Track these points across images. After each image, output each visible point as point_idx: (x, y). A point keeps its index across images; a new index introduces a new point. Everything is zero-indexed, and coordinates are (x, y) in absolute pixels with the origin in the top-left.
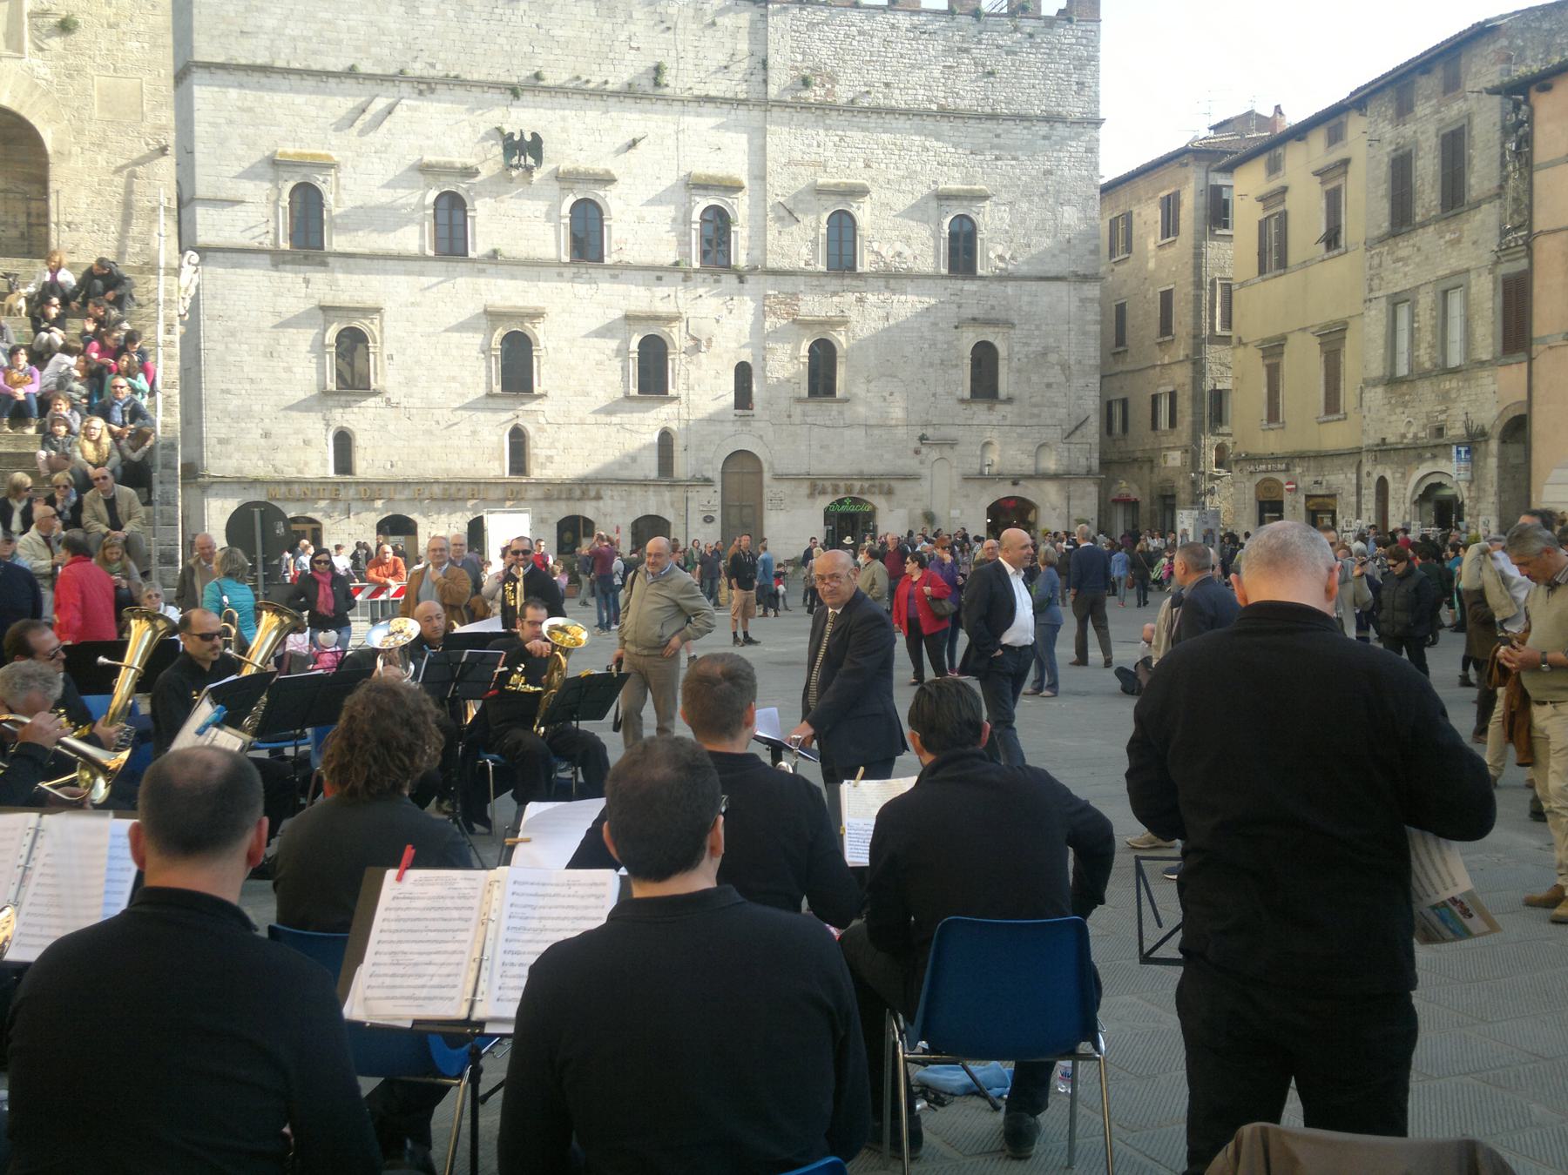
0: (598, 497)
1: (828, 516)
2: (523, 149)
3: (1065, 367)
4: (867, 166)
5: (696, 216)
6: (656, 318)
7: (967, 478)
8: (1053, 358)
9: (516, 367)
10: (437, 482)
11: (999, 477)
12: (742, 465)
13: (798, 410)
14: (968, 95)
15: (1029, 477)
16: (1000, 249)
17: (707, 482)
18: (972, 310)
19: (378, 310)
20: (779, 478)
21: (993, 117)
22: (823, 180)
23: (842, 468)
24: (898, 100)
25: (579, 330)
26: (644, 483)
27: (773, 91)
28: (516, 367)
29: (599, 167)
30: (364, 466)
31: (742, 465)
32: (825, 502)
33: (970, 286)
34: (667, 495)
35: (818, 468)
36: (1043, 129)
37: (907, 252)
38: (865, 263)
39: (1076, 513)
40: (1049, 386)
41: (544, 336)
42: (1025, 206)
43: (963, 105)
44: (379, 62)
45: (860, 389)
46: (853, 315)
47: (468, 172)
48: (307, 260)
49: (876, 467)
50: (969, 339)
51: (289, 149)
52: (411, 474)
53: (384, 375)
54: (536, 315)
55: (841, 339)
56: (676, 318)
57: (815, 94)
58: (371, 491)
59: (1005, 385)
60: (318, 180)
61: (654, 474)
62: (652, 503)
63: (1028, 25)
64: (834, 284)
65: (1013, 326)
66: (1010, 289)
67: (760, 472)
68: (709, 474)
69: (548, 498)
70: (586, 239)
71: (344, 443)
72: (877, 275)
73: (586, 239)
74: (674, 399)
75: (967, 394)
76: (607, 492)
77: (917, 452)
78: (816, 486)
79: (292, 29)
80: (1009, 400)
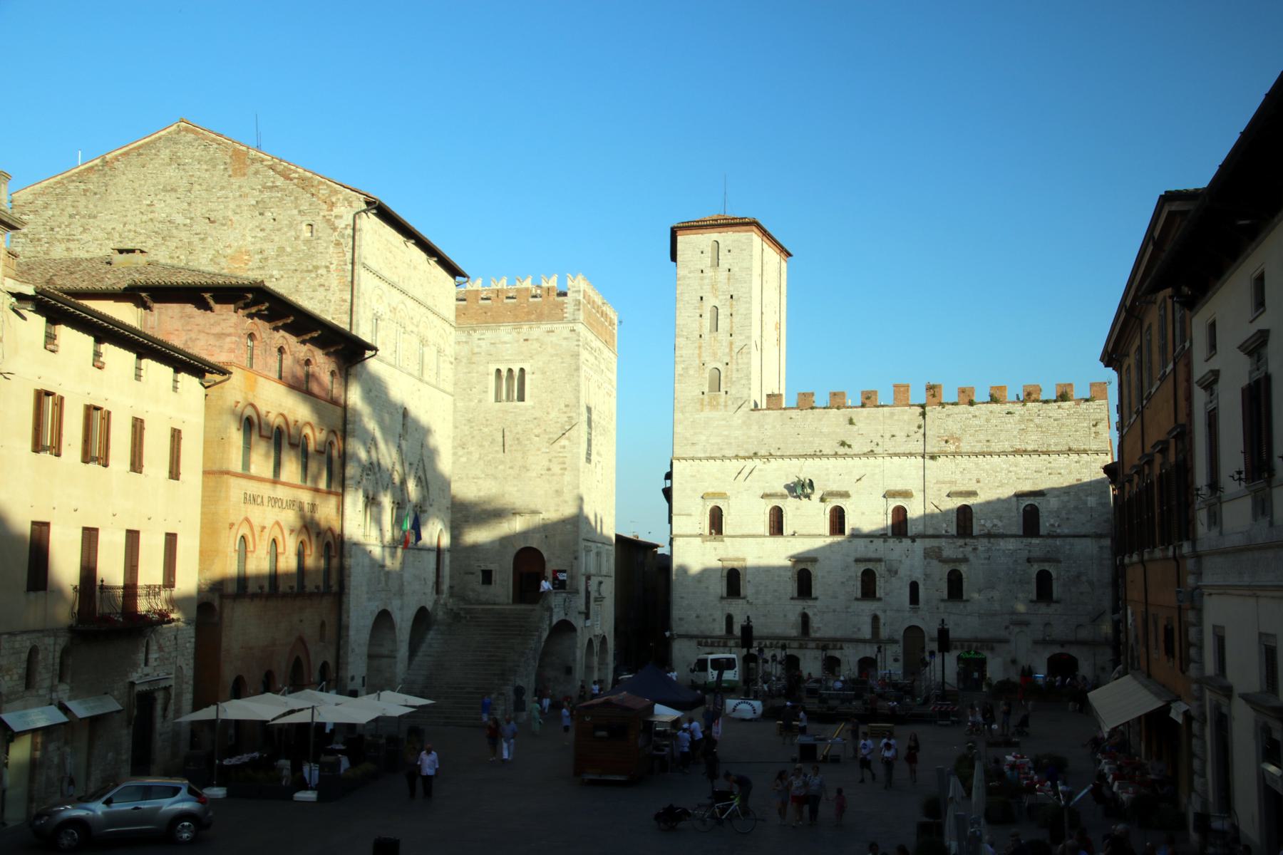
0: (841, 648)
4: (978, 482)
5: (890, 511)
6: (869, 560)
7: (1036, 642)
8: (1084, 578)
10: (767, 638)
11: (1053, 642)
12: (913, 634)
13: (942, 605)
15: (1071, 643)
16: (1052, 521)
17: (896, 642)
18: (1037, 553)
21: (1047, 453)
22: (954, 489)
24: (996, 447)
26: (864, 641)
27: (929, 449)
29: (843, 489)
33: (1035, 541)
37: (1000, 524)
38: (976, 531)
40: (1082, 593)
43: (1029, 448)
44: (747, 451)
45: (976, 596)
46: (971, 557)
50: (1036, 568)
51: (710, 490)
55: (963, 569)
56: (880, 560)
57: (951, 448)
59: (1057, 591)
60: (720, 503)
61: (868, 636)
62: (869, 651)
64: (961, 542)
65: (1059, 562)
66: (1058, 542)
67: (924, 637)
68: (897, 637)
71: (729, 619)
72: (984, 536)
74: (880, 599)
75: (1034, 598)
76: (845, 645)
77: (1007, 628)
79: (713, 440)
80: (1057, 602)
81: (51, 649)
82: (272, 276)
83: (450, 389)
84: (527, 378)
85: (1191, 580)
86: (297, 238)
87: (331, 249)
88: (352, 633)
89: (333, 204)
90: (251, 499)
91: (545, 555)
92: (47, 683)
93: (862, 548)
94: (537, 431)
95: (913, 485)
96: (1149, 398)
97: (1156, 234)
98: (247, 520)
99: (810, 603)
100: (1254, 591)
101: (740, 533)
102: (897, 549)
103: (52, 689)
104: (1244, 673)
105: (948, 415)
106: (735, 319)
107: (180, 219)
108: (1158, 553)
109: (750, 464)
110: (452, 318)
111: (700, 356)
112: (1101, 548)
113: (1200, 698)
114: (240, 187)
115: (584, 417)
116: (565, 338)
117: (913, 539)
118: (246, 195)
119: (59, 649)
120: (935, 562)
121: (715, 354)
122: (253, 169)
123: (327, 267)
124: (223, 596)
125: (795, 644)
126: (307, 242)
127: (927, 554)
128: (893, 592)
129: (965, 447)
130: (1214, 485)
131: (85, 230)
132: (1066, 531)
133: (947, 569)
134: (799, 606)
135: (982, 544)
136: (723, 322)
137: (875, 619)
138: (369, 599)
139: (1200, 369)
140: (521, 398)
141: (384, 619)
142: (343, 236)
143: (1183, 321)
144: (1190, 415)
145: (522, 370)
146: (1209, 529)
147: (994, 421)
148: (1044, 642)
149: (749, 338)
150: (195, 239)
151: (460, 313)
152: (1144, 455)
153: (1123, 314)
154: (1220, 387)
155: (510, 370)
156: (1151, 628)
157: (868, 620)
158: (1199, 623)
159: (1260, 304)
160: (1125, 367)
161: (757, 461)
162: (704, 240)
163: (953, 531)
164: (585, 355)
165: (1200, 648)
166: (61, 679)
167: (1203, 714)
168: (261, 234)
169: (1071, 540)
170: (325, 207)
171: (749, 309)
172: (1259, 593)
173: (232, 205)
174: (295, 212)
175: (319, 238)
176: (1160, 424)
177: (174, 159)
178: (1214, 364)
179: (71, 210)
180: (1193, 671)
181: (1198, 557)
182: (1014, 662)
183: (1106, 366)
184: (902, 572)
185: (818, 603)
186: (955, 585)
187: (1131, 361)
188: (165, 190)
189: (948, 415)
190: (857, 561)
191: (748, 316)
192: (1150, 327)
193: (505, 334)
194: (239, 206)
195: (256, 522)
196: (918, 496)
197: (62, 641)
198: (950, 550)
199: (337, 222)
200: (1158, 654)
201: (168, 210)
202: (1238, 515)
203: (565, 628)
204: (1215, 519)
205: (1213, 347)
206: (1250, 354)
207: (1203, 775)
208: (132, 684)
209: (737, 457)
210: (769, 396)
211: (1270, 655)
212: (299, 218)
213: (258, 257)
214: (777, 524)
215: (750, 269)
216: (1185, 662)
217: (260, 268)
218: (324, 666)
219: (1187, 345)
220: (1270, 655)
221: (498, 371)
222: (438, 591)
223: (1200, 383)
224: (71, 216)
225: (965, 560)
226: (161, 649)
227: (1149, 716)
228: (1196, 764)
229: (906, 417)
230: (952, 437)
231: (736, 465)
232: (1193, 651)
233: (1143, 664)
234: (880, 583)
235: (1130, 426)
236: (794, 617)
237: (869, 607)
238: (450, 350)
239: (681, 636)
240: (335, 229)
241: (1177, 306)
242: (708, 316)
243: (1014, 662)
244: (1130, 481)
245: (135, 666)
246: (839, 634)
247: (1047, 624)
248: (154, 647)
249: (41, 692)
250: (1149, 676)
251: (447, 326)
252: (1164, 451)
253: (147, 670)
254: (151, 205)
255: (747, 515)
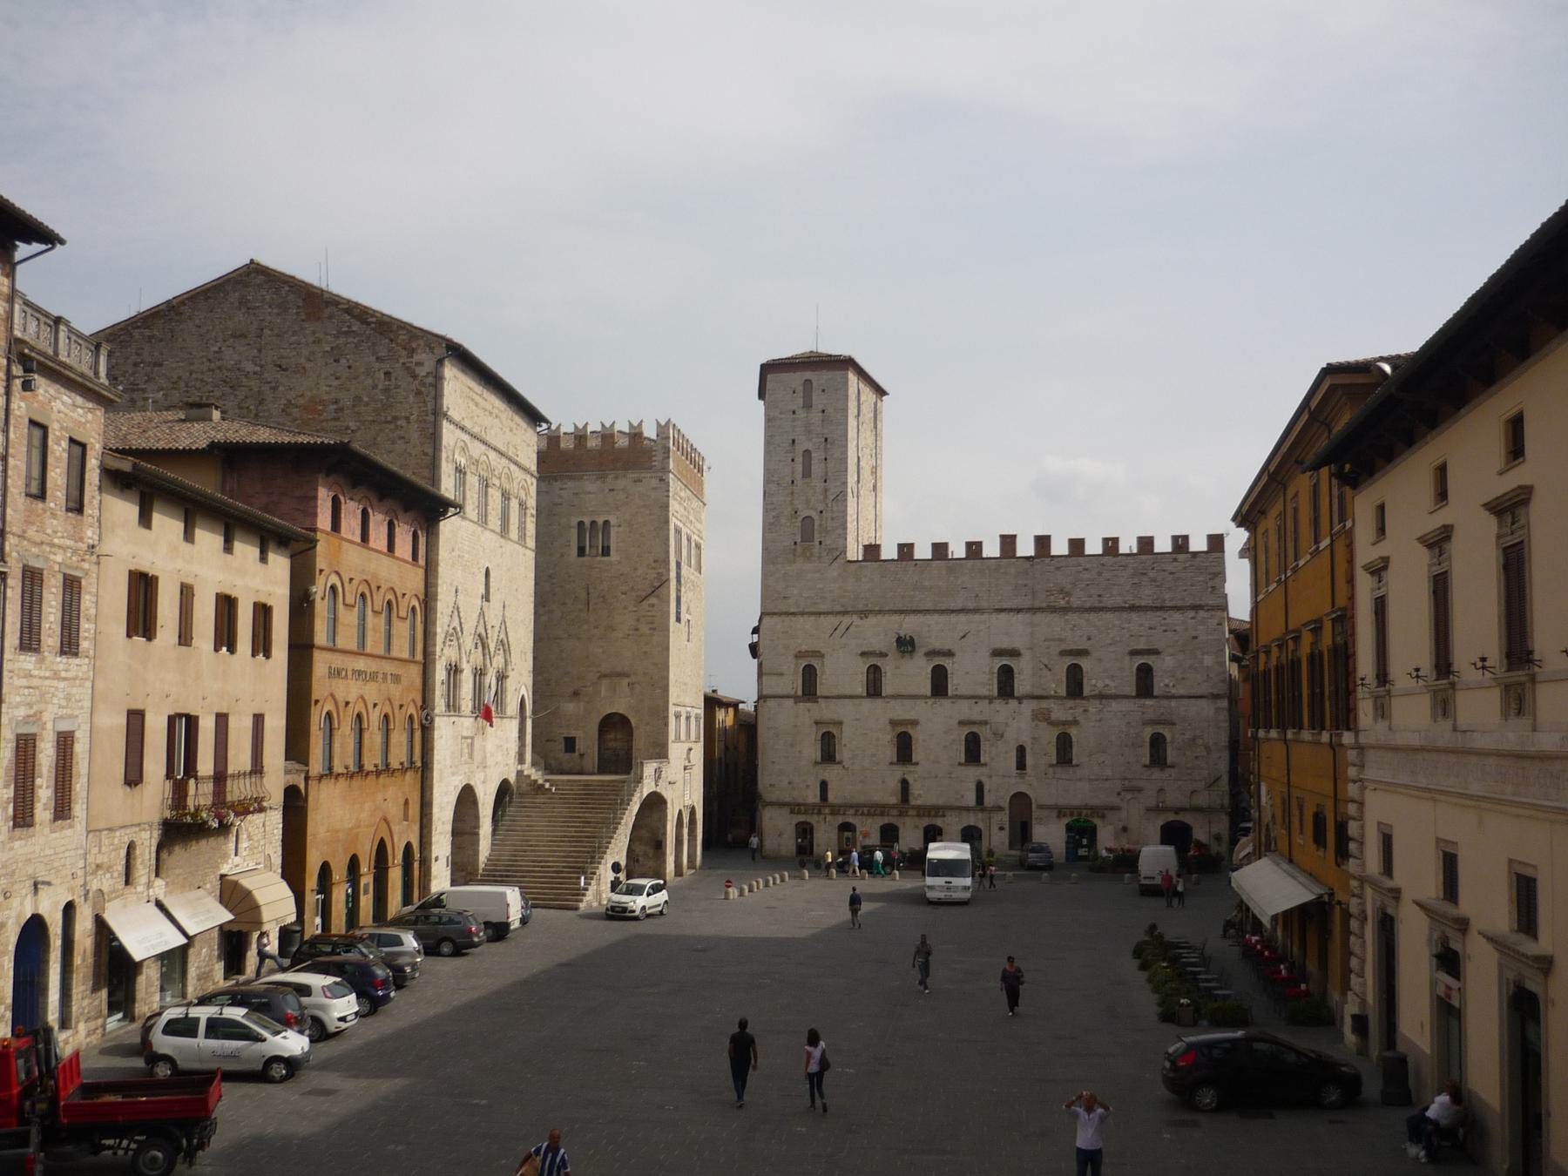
1: (1069, 828)
2: (906, 645)
3: (1207, 748)
6: (973, 723)
7: (1149, 810)
8: (1200, 742)
9: (904, 748)
10: (865, 806)
12: (1021, 802)
14: (1147, 596)
17: (1000, 809)
18: (1151, 715)
19: (841, 723)
20: (1041, 807)
21: (1161, 608)
22: (1064, 647)
23: (1076, 802)
24: (1109, 603)
25: (938, 729)
26: (967, 809)
28: (904, 748)
30: (831, 798)
31: (1021, 802)
32: (1067, 820)
33: (1149, 702)
34: (980, 815)
35: (1062, 802)
36: (1191, 614)
38: (1086, 692)
39: (1215, 830)
41: (918, 735)
42: (1181, 657)
43: (1143, 603)
46: (1081, 718)
47: (883, 655)
48: (809, 701)
49: (1096, 802)
50: (1148, 732)
51: (804, 648)
52: (854, 801)
53: (843, 753)
54: (915, 723)
55: (1073, 732)
56: (986, 723)
58: (836, 810)
59: (1171, 755)
60: (815, 663)
62: (971, 820)
63: (1181, 557)
64: (1070, 703)
66: (1173, 703)
69: (918, 815)
70: (939, 684)
71: (824, 786)
72: (1094, 697)
73: (939, 684)
76: (948, 813)
78: (1061, 812)
80: (1172, 766)
81: (148, 841)
82: (348, 428)
83: (531, 543)
84: (613, 531)
85: (1352, 772)
86: (375, 387)
87: (411, 399)
88: (435, 810)
89: (413, 350)
90: (336, 673)
91: (633, 722)
92: (144, 880)
93: (966, 710)
94: (624, 588)
95: (1018, 643)
96: (1295, 570)
97: (1313, 404)
98: (332, 695)
99: (911, 768)
100: (1433, 794)
101: (835, 692)
102: (1001, 712)
103: (149, 885)
104: (1417, 877)
105: (1058, 568)
106: (831, 464)
107: (249, 367)
108: (1306, 735)
109: (847, 620)
110: (534, 468)
111: (792, 503)
112: (1218, 709)
113: (1360, 896)
114: (314, 332)
115: (673, 575)
116: (654, 489)
117: (1020, 700)
118: (318, 341)
119: (155, 842)
120: (1043, 725)
121: (808, 502)
122: (327, 311)
123: (407, 419)
124: (307, 778)
125: (894, 812)
126: (386, 390)
127: (1039, 716)
128: (997, 756)
129: (1075, 602)
130: (1383, 677)
131: (149, 380)
132: (1182, 692)
133: (1055, 732)
134: (899, 771)
135: (1093, 706)
136: (817, 468)
137: (980, 788)
138: (453, 774)
139: (1365, 553)
140: (606, 551)
141: (467, 797)
142: (424, 385)
143: (1342, 498)
144: (1352, 598)
145: (606, 523)
146: (1375, 719)
147: (1106, 575)
148: (1157, 810)
149: (845, 483)
150: (266, 388)
151: (542, 458)
152: (1287, 631)
153: (1265, 478)
154: (1390, 575)
155: (593, 523)
156: (1295, 812)
157: (973, 787)
158: (1361, 818)
159: (1442, 495)
160: (1260, 530)
161: (855, 617)
162: (796, 379)
163: (1063, 691)
164: (674, 506)
165: (1362, 844)
166: (157, 875)
167: (1364, 912)
168: (336, 383)
169: (1186, 701)
170: (404, 353)
171: (845, 453)
172: (1437, 796)
173: (305, 352)
174: (373, 359)
175: (398, 387)
176: (1312, 602)
177: (243, 303)
178: (1383, 549)
179: (134, 358)
180: (1352, 866)
181: (1361, 748)
182: (1125, 829)
183: (1239, 526)
184: (1007, 735)
185: (918, 768)
186: (1064, 746)
187: (1270, 523)
188: (234, 336)
189: (1058, 568)
190: (961, 723)
191: (844, 460)
192: (1296, 495)
193: (590, 485)
194: (312, 353)
195: (340, 697)
196: (1027, 655)
197: (156, 834)
198: (1059, 713)
199: (418, 370)
200: (1304, 840)
201: (236, 357)
202: (1411, 714)
203: (655, 803)
204: (1382, 711)
205: (1382, 530)
206: (1430, 546)
207: (1361, 975)
208: (222, 876)
209: (831, 613)
210: (866, 547)
211: (1450, 864)
212: (377, 365)
213: (333, 407)
214: (874, 689)
215: (845, 410)
216: (1343, 854)
217: (336, 419)
218: (408, 846)
219: (1349, 524)
220: (1450, 864)
221: (581, 524)
222: (521, 760)
223: (1365, 568)
224: (136, 365)
225: (1075, 722)
226: (250, 838)
227: (1302, 909)
228: (1354, 962)
229: (1013, 570)
230: (1061, 591)
231: (833, 620)
232: (1352, 846)
233: (1283, 845)
234: (984, 746)
235: (1268, 595)
236: (893, 784)
237: (973, 773)
238: (532, 503)
239: (772, 804)
240: (415, 377)
241: (1335, 482)
242: (799, 459)
243: (1125, 829)
244: (1268, 653)
245: (225, 857)
246: (940, 802)
247: (1161, 790)
248: (243, 836)
249: (139, 889)
250: (1291, 861)
251: (528, 478)
252: (1317, 630)
253: (237, 860)
254: (220, 351)
255: (843, 673)
